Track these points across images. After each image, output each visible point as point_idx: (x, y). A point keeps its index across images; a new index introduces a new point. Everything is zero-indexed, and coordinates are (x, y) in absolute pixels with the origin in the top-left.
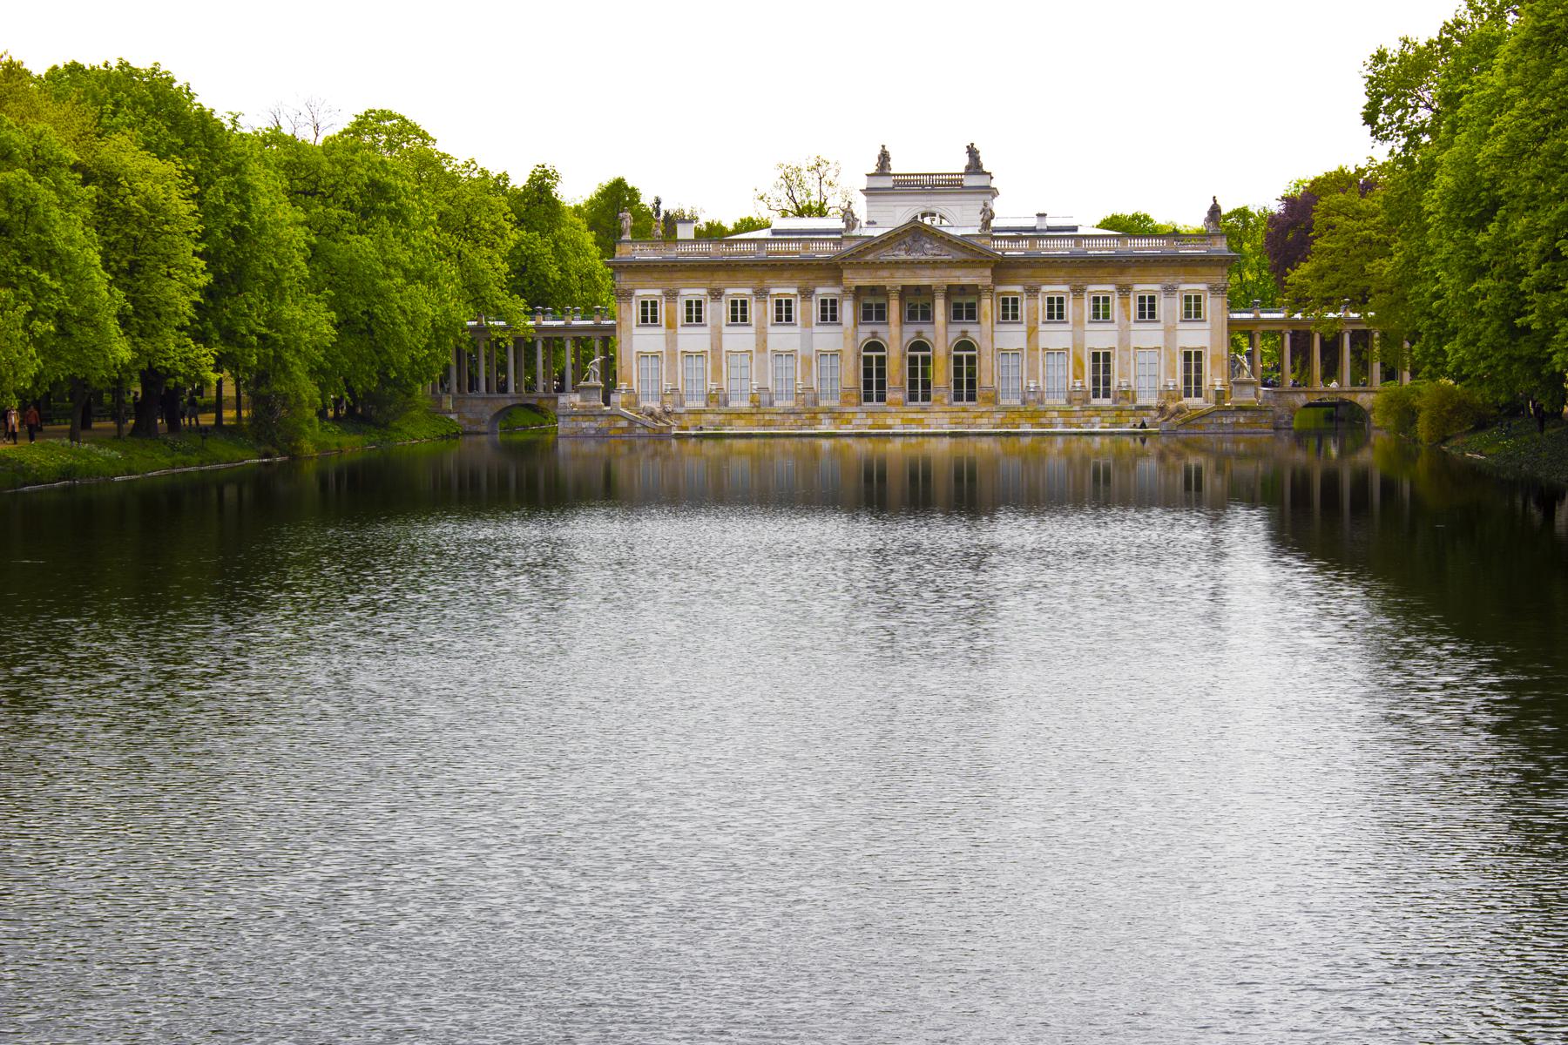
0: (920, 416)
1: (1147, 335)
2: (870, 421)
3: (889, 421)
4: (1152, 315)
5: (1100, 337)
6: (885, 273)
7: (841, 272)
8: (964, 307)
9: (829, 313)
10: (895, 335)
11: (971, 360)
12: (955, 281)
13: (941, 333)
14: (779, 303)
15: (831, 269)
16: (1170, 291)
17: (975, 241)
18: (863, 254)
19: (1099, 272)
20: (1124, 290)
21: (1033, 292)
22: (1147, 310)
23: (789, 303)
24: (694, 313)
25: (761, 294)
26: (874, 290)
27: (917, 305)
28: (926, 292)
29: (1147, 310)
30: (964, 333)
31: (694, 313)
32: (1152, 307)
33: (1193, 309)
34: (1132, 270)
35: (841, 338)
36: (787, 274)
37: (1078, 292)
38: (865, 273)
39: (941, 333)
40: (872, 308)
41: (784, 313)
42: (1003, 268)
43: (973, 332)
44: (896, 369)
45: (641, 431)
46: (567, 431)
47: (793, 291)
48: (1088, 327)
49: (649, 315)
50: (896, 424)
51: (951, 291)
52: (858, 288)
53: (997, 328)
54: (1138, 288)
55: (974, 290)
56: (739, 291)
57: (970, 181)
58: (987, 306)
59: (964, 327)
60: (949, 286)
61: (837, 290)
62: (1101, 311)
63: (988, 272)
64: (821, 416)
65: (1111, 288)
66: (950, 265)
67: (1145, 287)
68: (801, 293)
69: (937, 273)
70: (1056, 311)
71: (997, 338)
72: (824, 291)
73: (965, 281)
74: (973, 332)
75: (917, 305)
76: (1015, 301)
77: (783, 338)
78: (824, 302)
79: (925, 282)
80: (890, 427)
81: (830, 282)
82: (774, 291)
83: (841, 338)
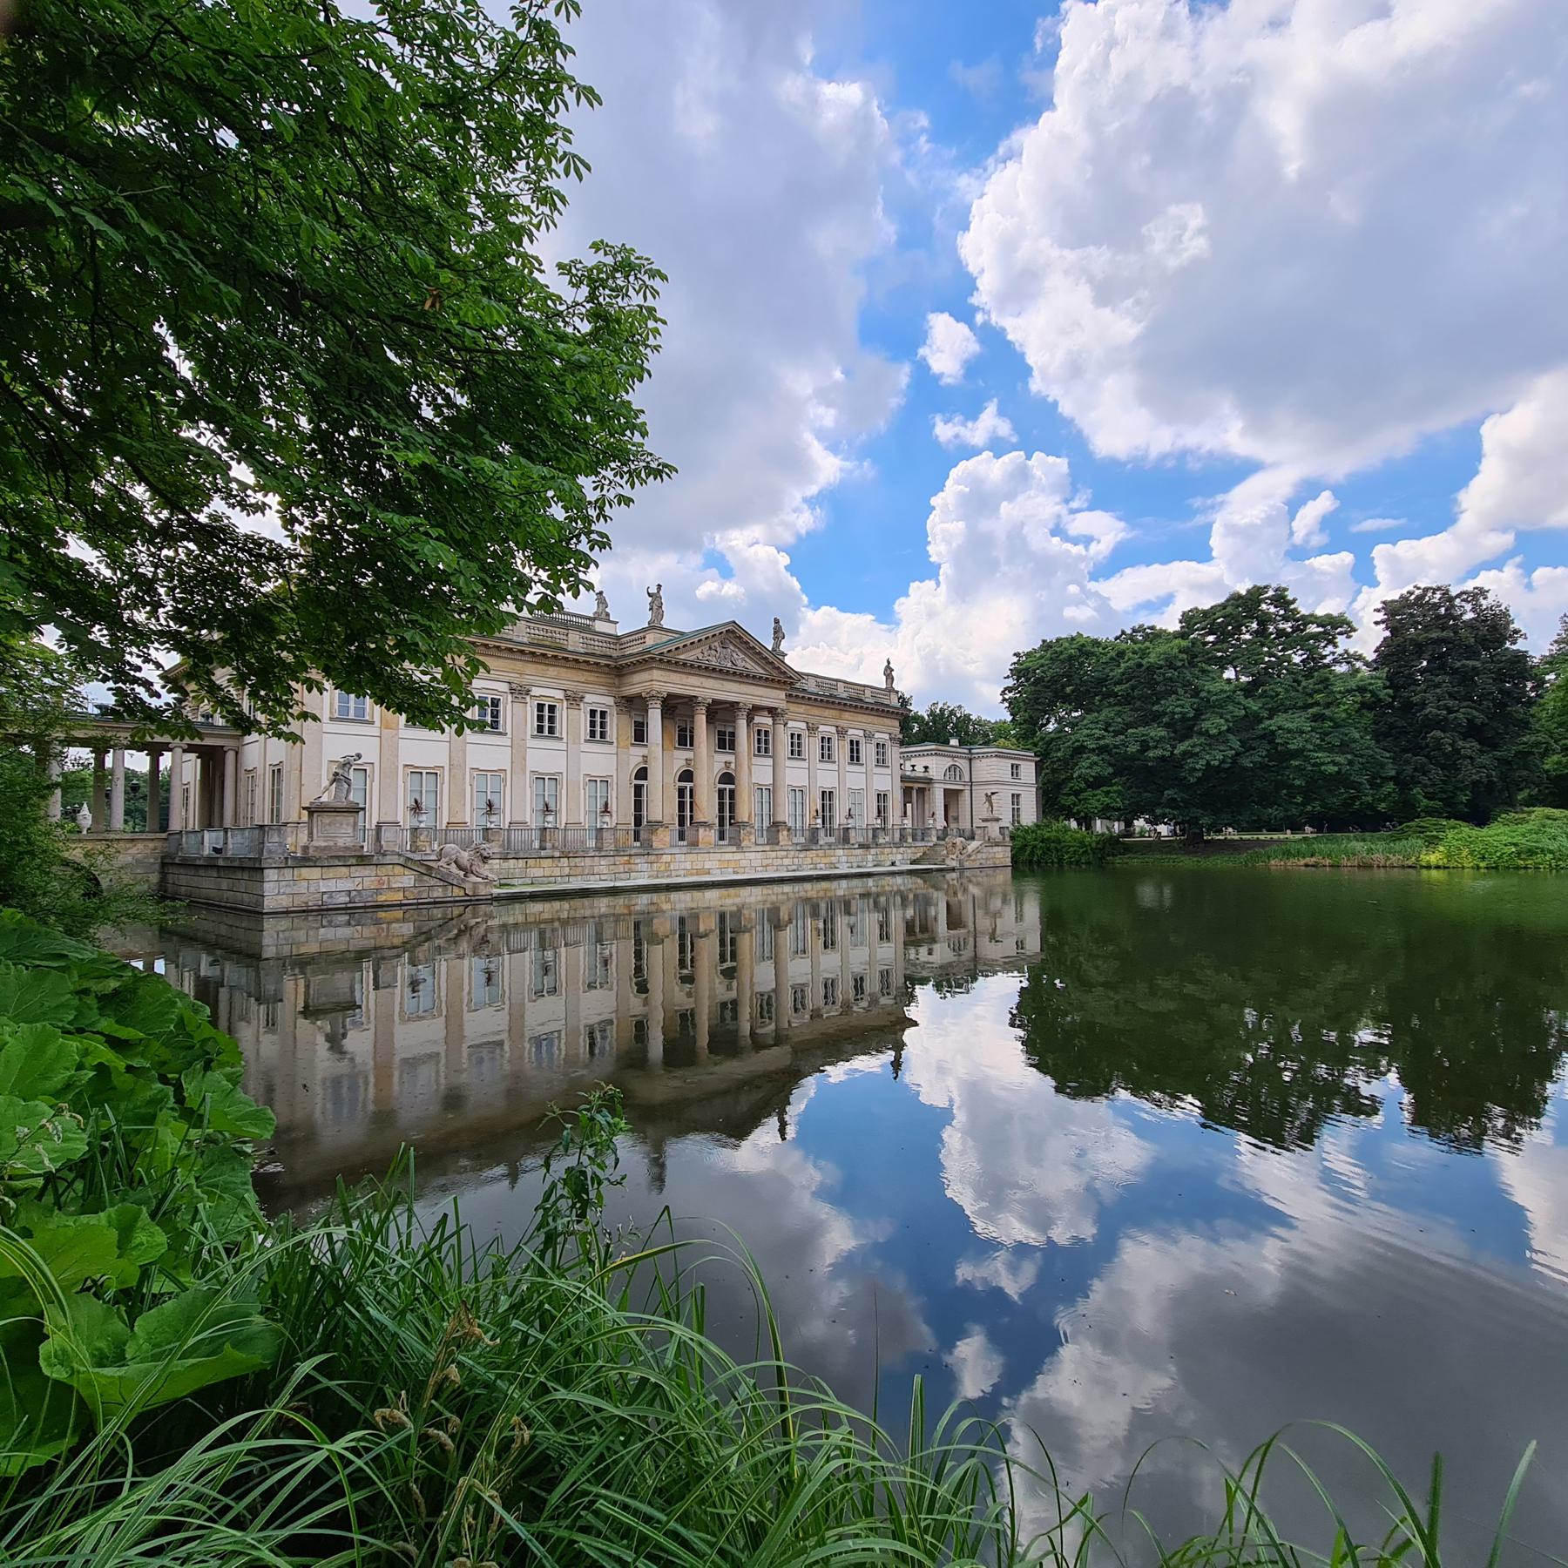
0: (738, 856)
1: (855, 778)
5: (826, 777)
6: (693, 680)
14: (540, 707)
19: (827, 713)
25: (519, 692)
36: (552, 671)
38: (675, 677)
39: (708, 762)
45: (438, 893)
46: (284, 902)
47: (560, 695)
53: (755, 760)
63: (782, 694)
77: (545, 756)
79: (732, 698)
81: (603, 690)
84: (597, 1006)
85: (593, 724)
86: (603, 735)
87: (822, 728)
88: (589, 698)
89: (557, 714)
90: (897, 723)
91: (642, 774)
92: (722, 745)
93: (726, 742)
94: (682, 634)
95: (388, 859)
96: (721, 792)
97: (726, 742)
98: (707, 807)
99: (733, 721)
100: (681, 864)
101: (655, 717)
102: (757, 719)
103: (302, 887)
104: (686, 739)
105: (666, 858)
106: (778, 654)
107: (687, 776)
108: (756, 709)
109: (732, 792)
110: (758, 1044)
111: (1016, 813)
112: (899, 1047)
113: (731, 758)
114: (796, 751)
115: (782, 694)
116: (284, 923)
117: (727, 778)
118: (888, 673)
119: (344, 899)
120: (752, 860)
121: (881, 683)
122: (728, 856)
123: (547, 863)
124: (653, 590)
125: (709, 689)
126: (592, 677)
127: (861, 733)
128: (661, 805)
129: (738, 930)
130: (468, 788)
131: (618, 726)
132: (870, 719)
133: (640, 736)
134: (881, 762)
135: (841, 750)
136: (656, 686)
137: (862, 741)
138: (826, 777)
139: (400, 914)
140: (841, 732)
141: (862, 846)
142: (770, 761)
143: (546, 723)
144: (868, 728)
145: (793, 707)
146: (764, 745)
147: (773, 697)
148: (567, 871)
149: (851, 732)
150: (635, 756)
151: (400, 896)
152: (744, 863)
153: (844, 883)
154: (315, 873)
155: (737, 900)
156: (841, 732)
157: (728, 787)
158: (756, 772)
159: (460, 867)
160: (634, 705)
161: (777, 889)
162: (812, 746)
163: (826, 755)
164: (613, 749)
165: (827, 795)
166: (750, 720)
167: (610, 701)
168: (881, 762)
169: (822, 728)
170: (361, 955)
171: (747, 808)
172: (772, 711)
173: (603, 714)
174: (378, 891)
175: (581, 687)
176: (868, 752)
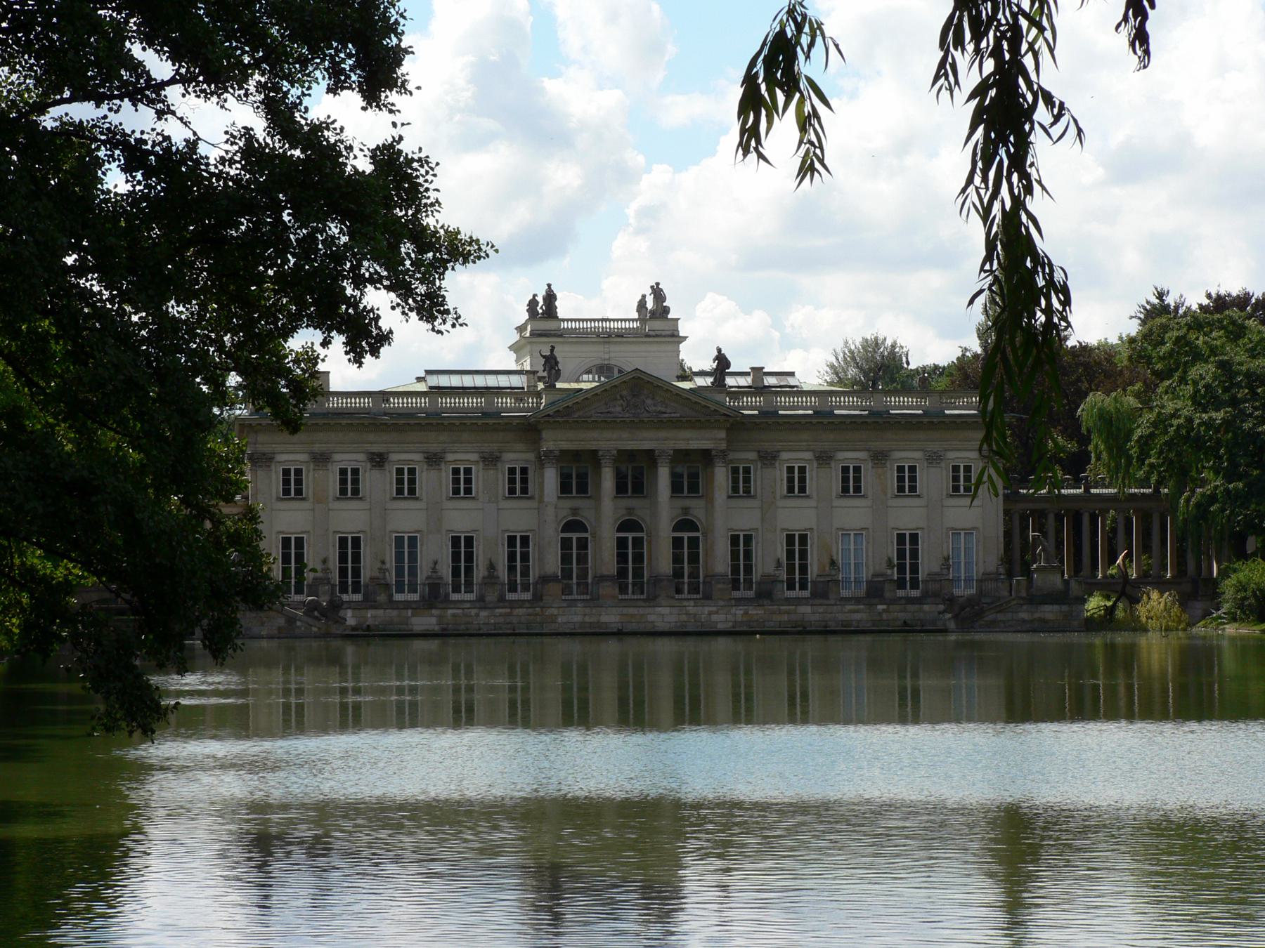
0: (641, 611)
2: (578, 619)
3: (604, 619)
4: (913, 489)
6: (595, 434)
7: (539, 432)
8: (691, 473)
9: (519, 485)
10: (606, 510)
11: (638, 542)
12: (682, 445)
13: (663, 508)
15: (529, 429)
16: (934, 459)
17: (707, 395)
18: (571, 411)
20: (879, 458)
21: (769, 458)
22: (907, 482)
23: (468, 471)
24: (350, 485)
25: (434, 460)
26: (576, 455)
27: (634, 475)
28: (650, 457)
29: (907, 482)
30: (686, 510)
31: (350, 485)
32: (913, 479)
33: (963, 484)
35: (542, 516)
37: (824, 459)
40: (577, 474)
41: (462, 485)
42: (737, 425)
43: (697, 509)
44: (604, 556)
48: (837, 502)
49: (292, 486)
50: (611, 618)
51: (682, 456)
52: (563, 452)
54: (897, 455)
55: (707, 457)
56: (406, 456)
57: (658, 325)
58: (721, 476)
59: (688, 503)
60: (676, 451)
61: (531, 456)
62: (851, 484)
63: (723, 434)
65: (862, 455)
66: (676, 424)
67: (907, 455)
68: (484, 459)
69: (663, 434)
70: (797, 485)
71: (725, 516)
72: (516, 457)
73: (695, 445)
74: (697, 509)
75: (634, 475)
76: (747, 470)
78: (512, 471)
79: (647, 445)
81: (521, 446)
82: (450, 457)
83: (542, 516)
88: (508, 456)
125: (608, 441)
143: (462, 485)
146: (741, 486)
152: (651, 618)
169: (841, 455)
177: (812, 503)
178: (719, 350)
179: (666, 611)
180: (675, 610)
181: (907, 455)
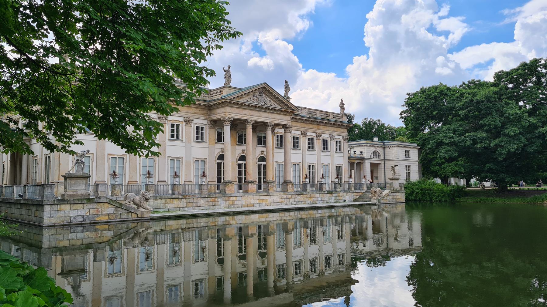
0: (267, 197)
1: (325, 158)
3: (253, 202)
5: (311, 158)
6: (246, 112)
19: (311, 126)
34: (321, 127)
38: (237, 110)
39: (253, 151)
45: (125, 216)
46: (53, 221)
53: (276, 150)
63: (289, 118)
64: (219, 199)
78: (197, 128)
79: (264, 120)
80: (253, 205)
81: (202, 117)
84: (199, 270)
85: (197, 133)
86: (202, 139)
87: (309, 134)
88: (195, 121)
89: (180, 129)
90: (346, 131)
91: (221, 157)
92: (259, 143)
93: (261, 141)
94: (240, 89)
95: (101, 200)
96: (259, 166)
97: (261, 141)
98: (252, 173)
99: (265, 131)
100: (240, 202)
101: (227, 130)
102: (277, 130)
103: (61, 214)
104: (242, 140)
105: (232, 199)
106: (286, 97)
107: (243, 158)
108: (276, 125)
109: (264, 166)
110: (278, 291)
111: (408, 175)
112: (348, 294)
113: (264, 149)
114: (296, 145)
115: (289, 118)
116: (53, 231)
117: (262, 159)
118: (342, 105)
119: (80, 219)
120: (274, 200)
121: (338, 111)
122: (263, 198)
123: (175, 201)
124: (226, 68)
126: (197, 111)
127: (328, 136)
128: (230, 173)
129: (267, 234)
130: (138, 165)
131: (209, 134)
132: (333, 129)
133: (220, 138)
134: (338, 150)
135: (318, 145)
136: (228, 115)
137: (329, 140)
138: (311, 158)
139: (107, 227)
140: (318, 136)
141: (329, 192)
142: (283, 151)
144: (332, 133)
145: (294, 124)
146: (280, 142)
147: (285, 119)
148: (185, 205)
149: (323, 135)
150: (218, 148)
151: (106, 218)
152: (270, 201)
153: (320, 211)
154: (67, 207)
155: (268, 219)
156: (318, 136)
157: (263, 163)
158: (277, 156)
159: (135, 204)
160: (217, 124)
161: (287, 214)
162: (304, 143)
163: (311, 147)
164: (206, 145)
165: (311, 167)
166: (273, 130)
167: (205, 122)
168: (338, 150)
169: (309, 134)
170: (88, 246)
171: (272, 174)
172: (284, 126)
173: (202, 128)
174: (97, 216)
175: (192, 116)
176: (332, 145)
177: (300, 152)
178: (286, 82)
179: (274, 197)
180: (278, 197)
181: (325, 136)
